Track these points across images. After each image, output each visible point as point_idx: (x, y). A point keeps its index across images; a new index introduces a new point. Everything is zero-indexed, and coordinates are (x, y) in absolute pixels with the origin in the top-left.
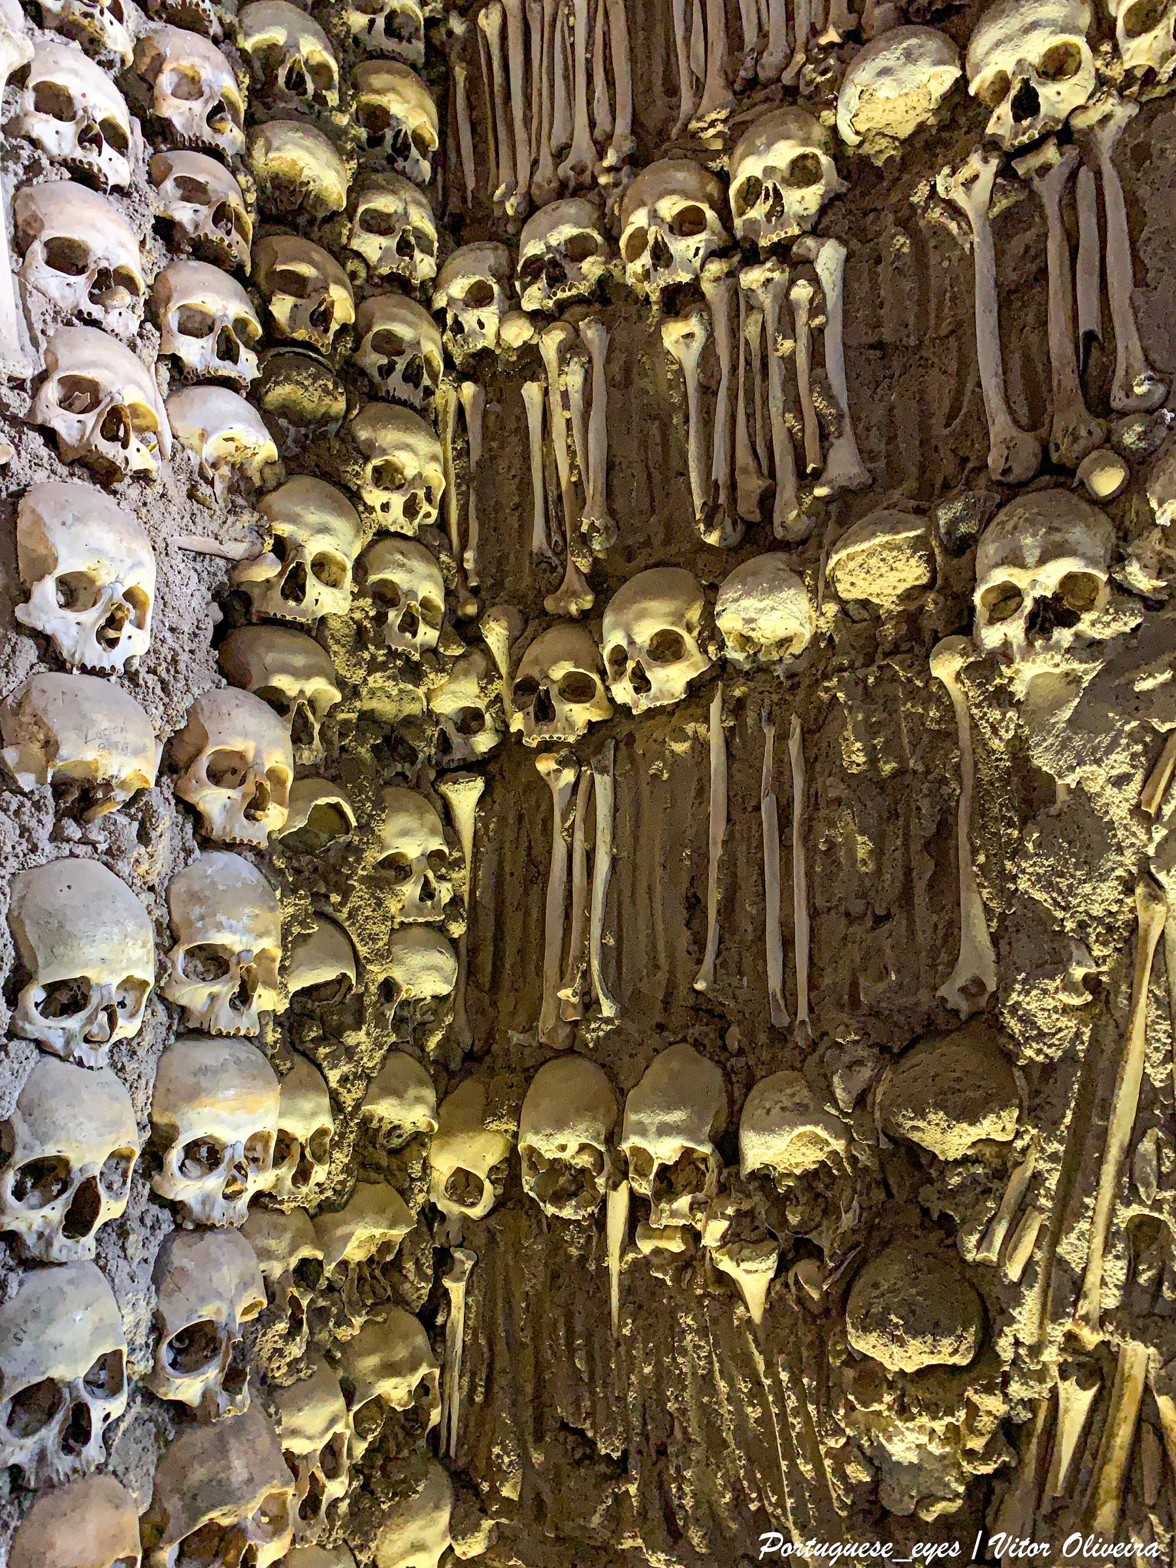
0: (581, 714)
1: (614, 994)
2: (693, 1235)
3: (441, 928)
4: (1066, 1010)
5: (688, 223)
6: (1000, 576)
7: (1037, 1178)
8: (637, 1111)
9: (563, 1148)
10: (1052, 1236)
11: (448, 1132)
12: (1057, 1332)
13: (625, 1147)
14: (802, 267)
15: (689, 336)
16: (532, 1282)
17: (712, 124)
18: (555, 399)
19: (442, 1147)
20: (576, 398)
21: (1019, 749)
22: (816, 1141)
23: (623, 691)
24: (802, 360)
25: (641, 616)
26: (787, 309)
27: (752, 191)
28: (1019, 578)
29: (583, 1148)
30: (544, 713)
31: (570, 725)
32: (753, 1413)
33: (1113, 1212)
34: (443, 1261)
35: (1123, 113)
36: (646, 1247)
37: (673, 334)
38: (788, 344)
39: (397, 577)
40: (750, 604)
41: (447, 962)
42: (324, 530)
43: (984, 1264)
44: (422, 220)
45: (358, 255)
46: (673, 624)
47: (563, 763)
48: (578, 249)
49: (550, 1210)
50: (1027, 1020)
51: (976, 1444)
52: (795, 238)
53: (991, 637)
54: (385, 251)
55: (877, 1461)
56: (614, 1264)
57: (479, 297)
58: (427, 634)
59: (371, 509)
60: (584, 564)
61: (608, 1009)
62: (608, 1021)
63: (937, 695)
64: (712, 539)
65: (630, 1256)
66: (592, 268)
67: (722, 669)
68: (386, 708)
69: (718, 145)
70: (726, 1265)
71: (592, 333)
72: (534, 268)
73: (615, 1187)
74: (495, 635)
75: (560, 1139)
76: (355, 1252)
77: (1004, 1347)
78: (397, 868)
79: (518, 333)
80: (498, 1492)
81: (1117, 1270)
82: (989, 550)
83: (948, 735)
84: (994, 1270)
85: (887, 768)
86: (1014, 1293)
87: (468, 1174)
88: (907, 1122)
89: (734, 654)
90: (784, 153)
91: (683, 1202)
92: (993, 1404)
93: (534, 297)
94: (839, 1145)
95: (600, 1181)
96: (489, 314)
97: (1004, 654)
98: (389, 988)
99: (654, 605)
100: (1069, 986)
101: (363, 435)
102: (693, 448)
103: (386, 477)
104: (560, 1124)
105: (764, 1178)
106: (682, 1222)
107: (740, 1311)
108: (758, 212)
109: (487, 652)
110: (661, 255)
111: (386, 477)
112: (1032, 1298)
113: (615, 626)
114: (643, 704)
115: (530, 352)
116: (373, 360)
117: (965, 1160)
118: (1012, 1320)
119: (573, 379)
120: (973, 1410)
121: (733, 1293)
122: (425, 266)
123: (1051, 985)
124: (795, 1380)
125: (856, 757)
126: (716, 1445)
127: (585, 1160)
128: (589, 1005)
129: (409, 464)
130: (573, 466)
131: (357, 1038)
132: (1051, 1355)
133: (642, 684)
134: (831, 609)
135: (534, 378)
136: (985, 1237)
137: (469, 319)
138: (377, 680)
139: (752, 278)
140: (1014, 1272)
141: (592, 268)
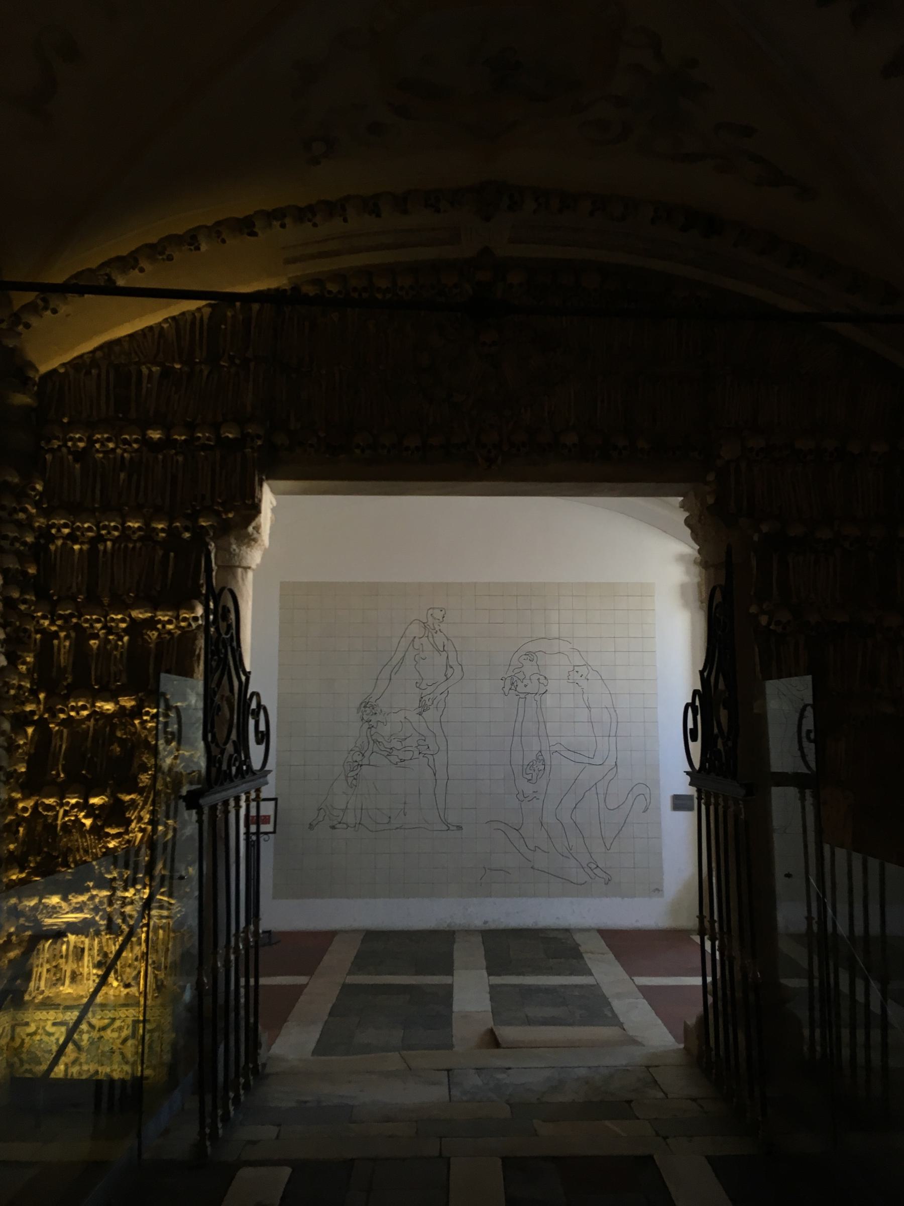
0: (62, 716)
1: (64, 772)
2: (76, 816)
3: (24, 758)
4: (147, 778)
5: (98, 621)
6: (147, 709)
7: (139, 804)
8: (68, 794)
9: (50, 801)
10: (139, 812)
11: (25, 798)
12: (138, 826)
13: (64, 801)
14: (121, 639)
15: (95, 643)
16: (39, 828)
17: (106, 600)
18: (62, 646)
19: (21, 802)
20: (67, 647)
21: (146, 736)
22: (102, 799)
23: (73, 714)
24: (118, 656)
25: (79, 701)
26: (117, 645)
27: (113, 620)
28: (150, 710)
29: (54, 802)
30: (54, 715)
31: (59, 717)
32: (85, 844)
33: (149, 808)
34: (19, 825)
35: (179, 632)
36: (67, 819)
37: (92, 642)
38: (115, 653)
39: (23, 683)
40: (103, 703)
41: (25, 765)
42: (14, 679)
43: (129, 817)
44: (34, 598)
45: (20, 609)
46: (86, 703)
47: (57, 725)
48: (71, 615)
49: (45, 813)
50: (141, 779)
51: (123, 843)
52: (120, 632)
53: (145, 718)
54: (26, 608)
55: (107, 848)
56: (59, 822)
57: (44, 617)
58: (27, 694)
59: (19, 669)
60: (65, 684)
61: (62, 775)
62: (62, 778)
63: (134, 725)
64: (96, 687)
65: (63, 821)
66: (74, 620)
67: (95, 712)
68: (17, 711)
69: (106, 604)
70: (84, 821)
71: (73, 634)
72: (61, 617)
73: (61, 808)
74: (42, 696)
75: (50, 800)
76: (7, 821)
77: (130, 829)
78: (19, 746)
79: (54, 628)
80: (29, 865)
81: (148, 816)
82: (146, 704)
83: (135, 733)
84: (130, 818)
85: (124, 736)
86: (132, 821)
87: (25, 807)
88: (119, 795)
89: (98, 710)
90: (120, 616)
91: (76, 810)
92: (127, 837)
93: (59, 622)
94: (107, 799)
95: (58, 808)
96: (46, 623)
97: (146, 721)
98: (15, 770)
99: (83, 699)
100: (148, 775)
101: (19, 653)
102: (93, 667)
103: (24, 663)
104: (51, 797)
105: (93, 805)
106: (75, 814)
107: (85, 828)
108: (113, 624)
109: (38, 698)
110: (92, 627)
111: (24, 663)
112: (135, 822)
113: (73, 701)
114: (78, 717)
115: (56, 632)
116: (22, 634)
117: (128, 801)
118: (131, 825)
119: (67, 643)
120: (124, 838)
121: (84, 825)
122: (33, 608)
123: (145, 774)
124: (94, 838)
125: (119, 734)
126: (78, 850)
127: (55, 804)
128: (58, 775)
129: (28, 659)
130: (65, 662)
131: (12, 780)
132: (136, 829)
133: (78, 713)
134: (118, 706)
135: (57, 639)
136: (129, 814)
137: (42, 621)
138: (17, 706)
139: (111, 637)
140: (133, 818)
141: (74, 620)
